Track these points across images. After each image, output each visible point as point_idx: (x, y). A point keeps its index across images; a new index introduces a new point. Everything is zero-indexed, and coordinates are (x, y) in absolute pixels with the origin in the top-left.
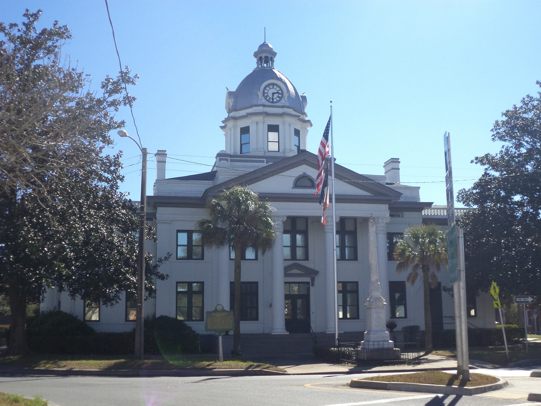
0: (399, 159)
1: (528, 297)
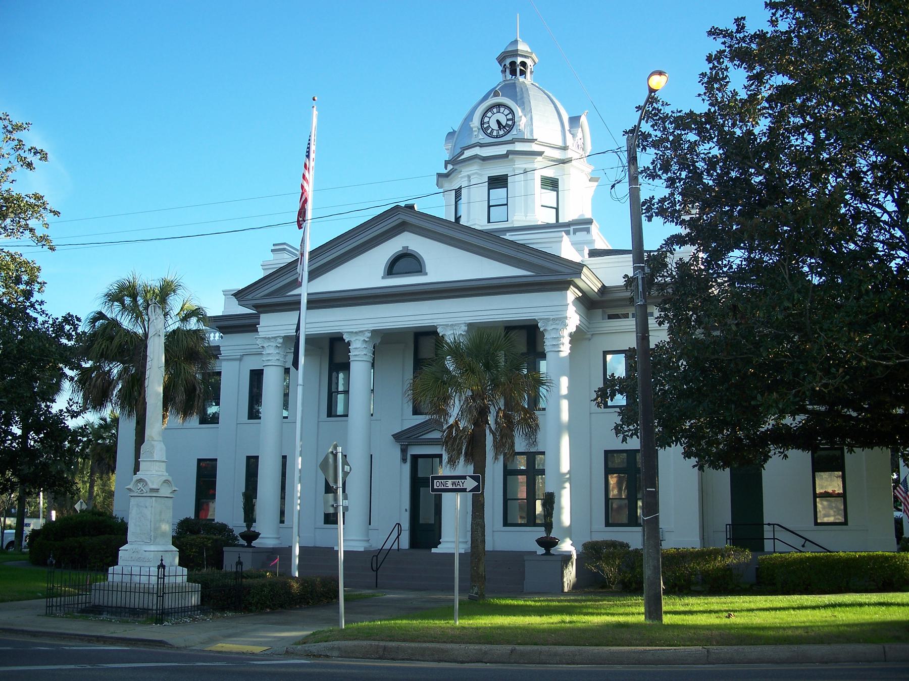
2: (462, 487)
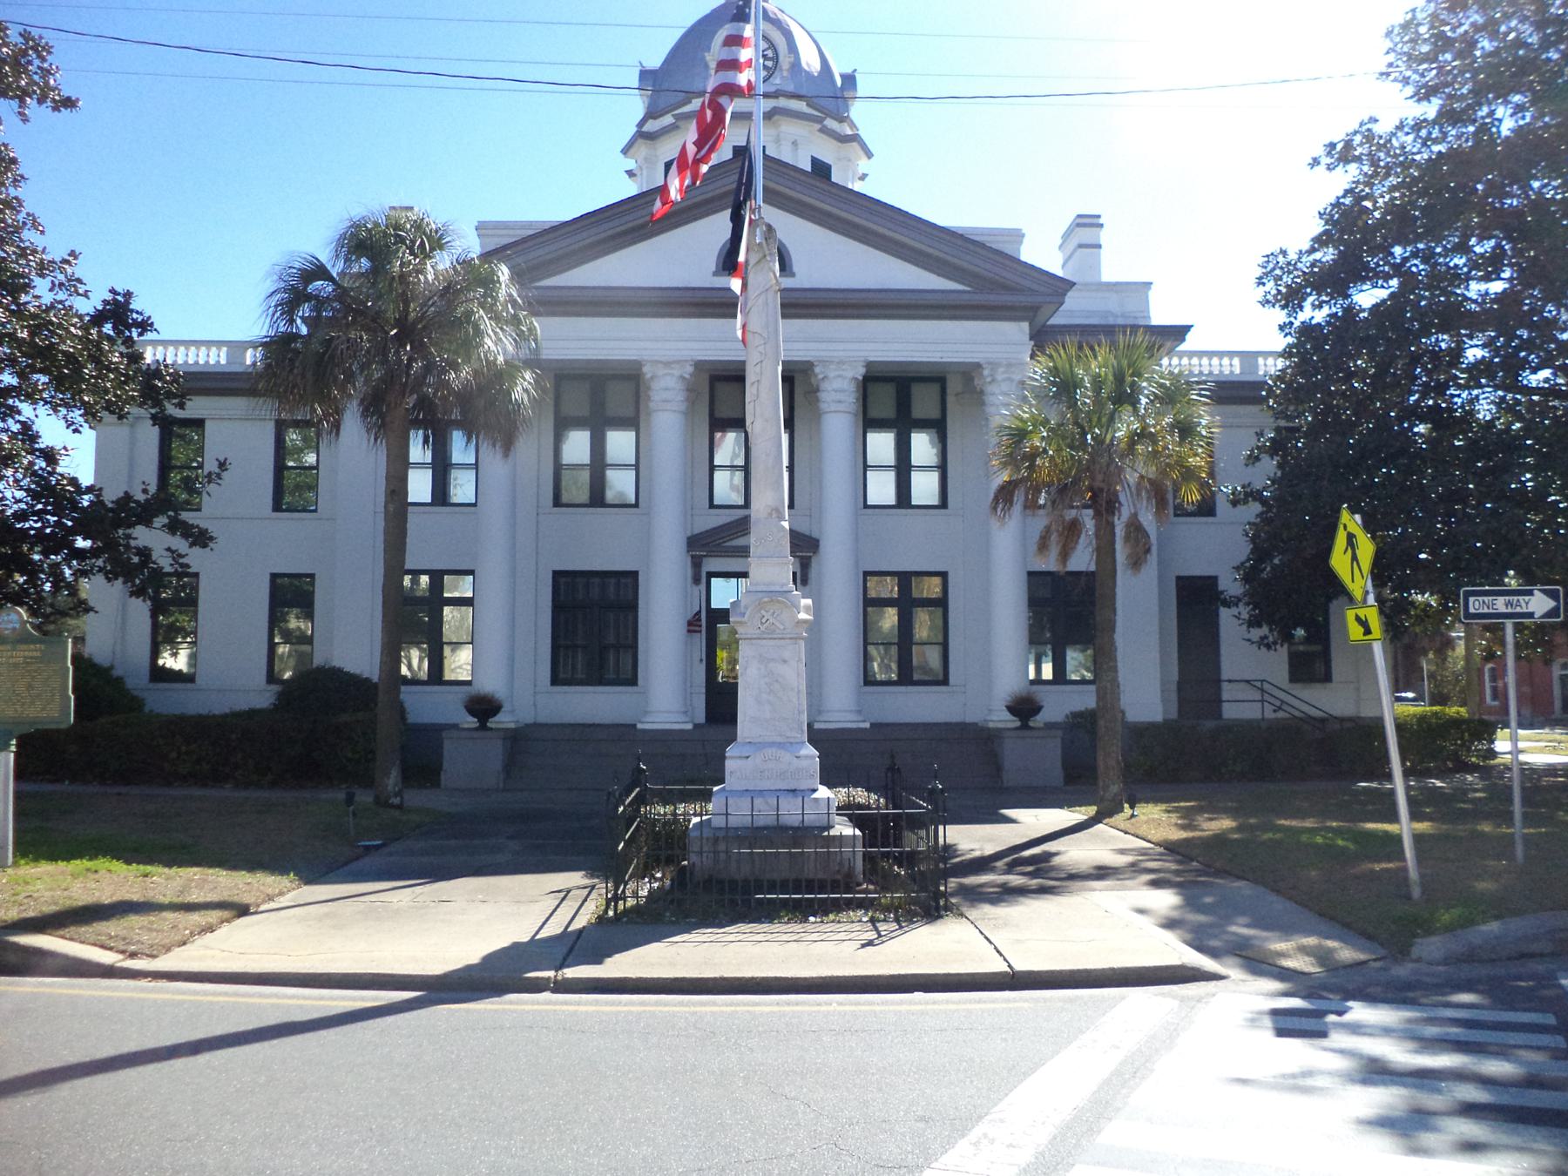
0: (1099, 216)
1: (1530, 593)
2: (1525, 610)
